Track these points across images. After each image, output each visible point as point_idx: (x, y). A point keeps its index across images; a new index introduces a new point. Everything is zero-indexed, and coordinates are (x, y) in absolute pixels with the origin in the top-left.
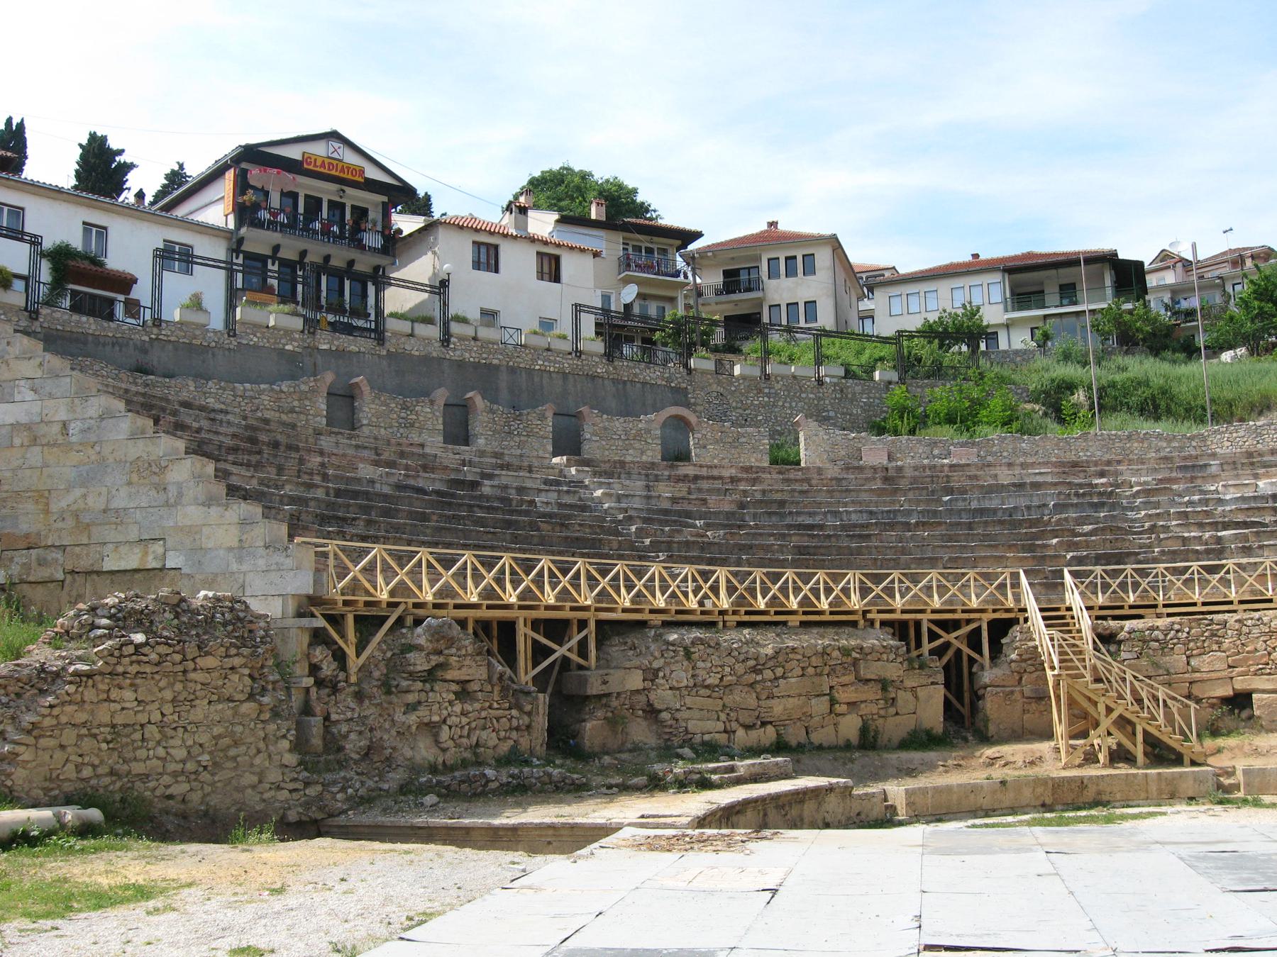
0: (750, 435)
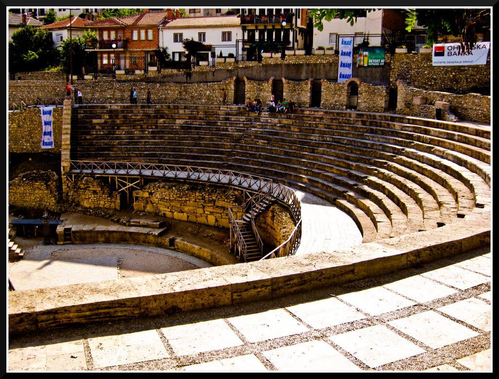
0: (379, 89)
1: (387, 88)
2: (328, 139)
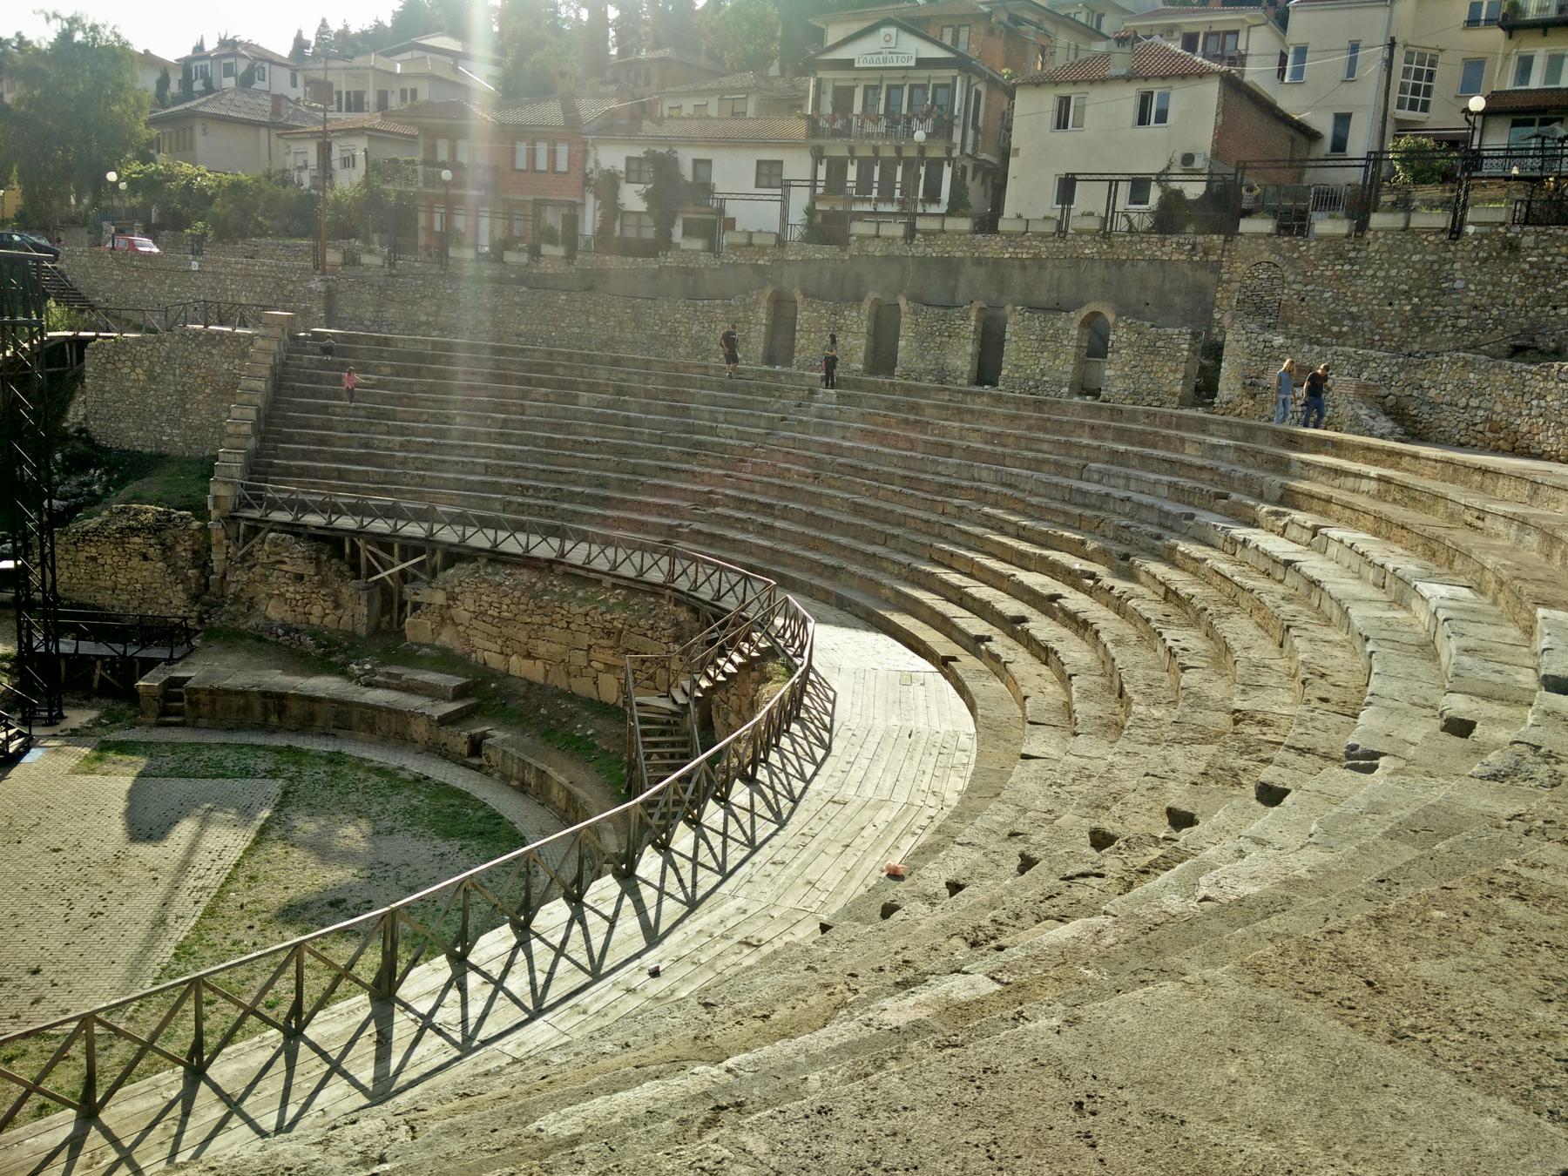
1: (1195, 335)
2: (984, 475)
